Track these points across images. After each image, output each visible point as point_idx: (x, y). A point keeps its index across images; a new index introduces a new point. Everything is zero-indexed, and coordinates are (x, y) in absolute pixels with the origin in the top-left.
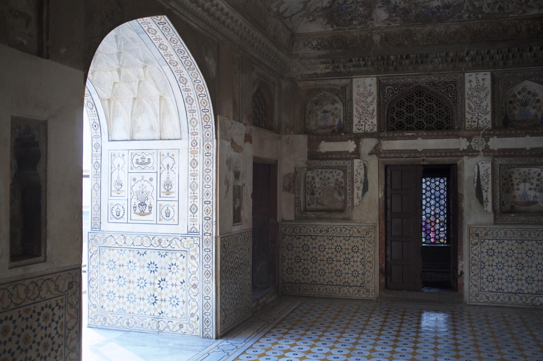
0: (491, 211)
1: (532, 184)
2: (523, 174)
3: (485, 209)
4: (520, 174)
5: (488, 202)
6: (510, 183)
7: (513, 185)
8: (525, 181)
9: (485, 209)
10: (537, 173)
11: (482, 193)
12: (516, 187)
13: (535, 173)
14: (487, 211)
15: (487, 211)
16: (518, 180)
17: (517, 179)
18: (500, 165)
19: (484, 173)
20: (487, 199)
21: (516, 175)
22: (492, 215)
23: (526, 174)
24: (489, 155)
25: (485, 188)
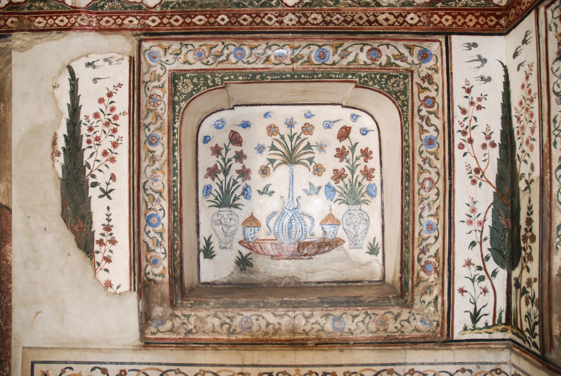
0: (125, 287)
1: (318, 170)
2: (284, 130)
3: (102, 276)
4: (272, 130)
5: (113, 242)
6: (236, 166)
7: (244, 173)
8: (291, 159)
9: (102, 276)
10: (336, 128)
11: (86, 200)
12: (256, 182)
13: (328, 125)
14: (108, 284)
15: (108, 284)
16: (267, 153)
17: (260, 149)
18: (175, 77)
19: (97, 107)
20: (108, 228)
21: (256, 136)
22: (132, 303)
23: (297, 129)
24: (120, 29)
25: (102, 178)
